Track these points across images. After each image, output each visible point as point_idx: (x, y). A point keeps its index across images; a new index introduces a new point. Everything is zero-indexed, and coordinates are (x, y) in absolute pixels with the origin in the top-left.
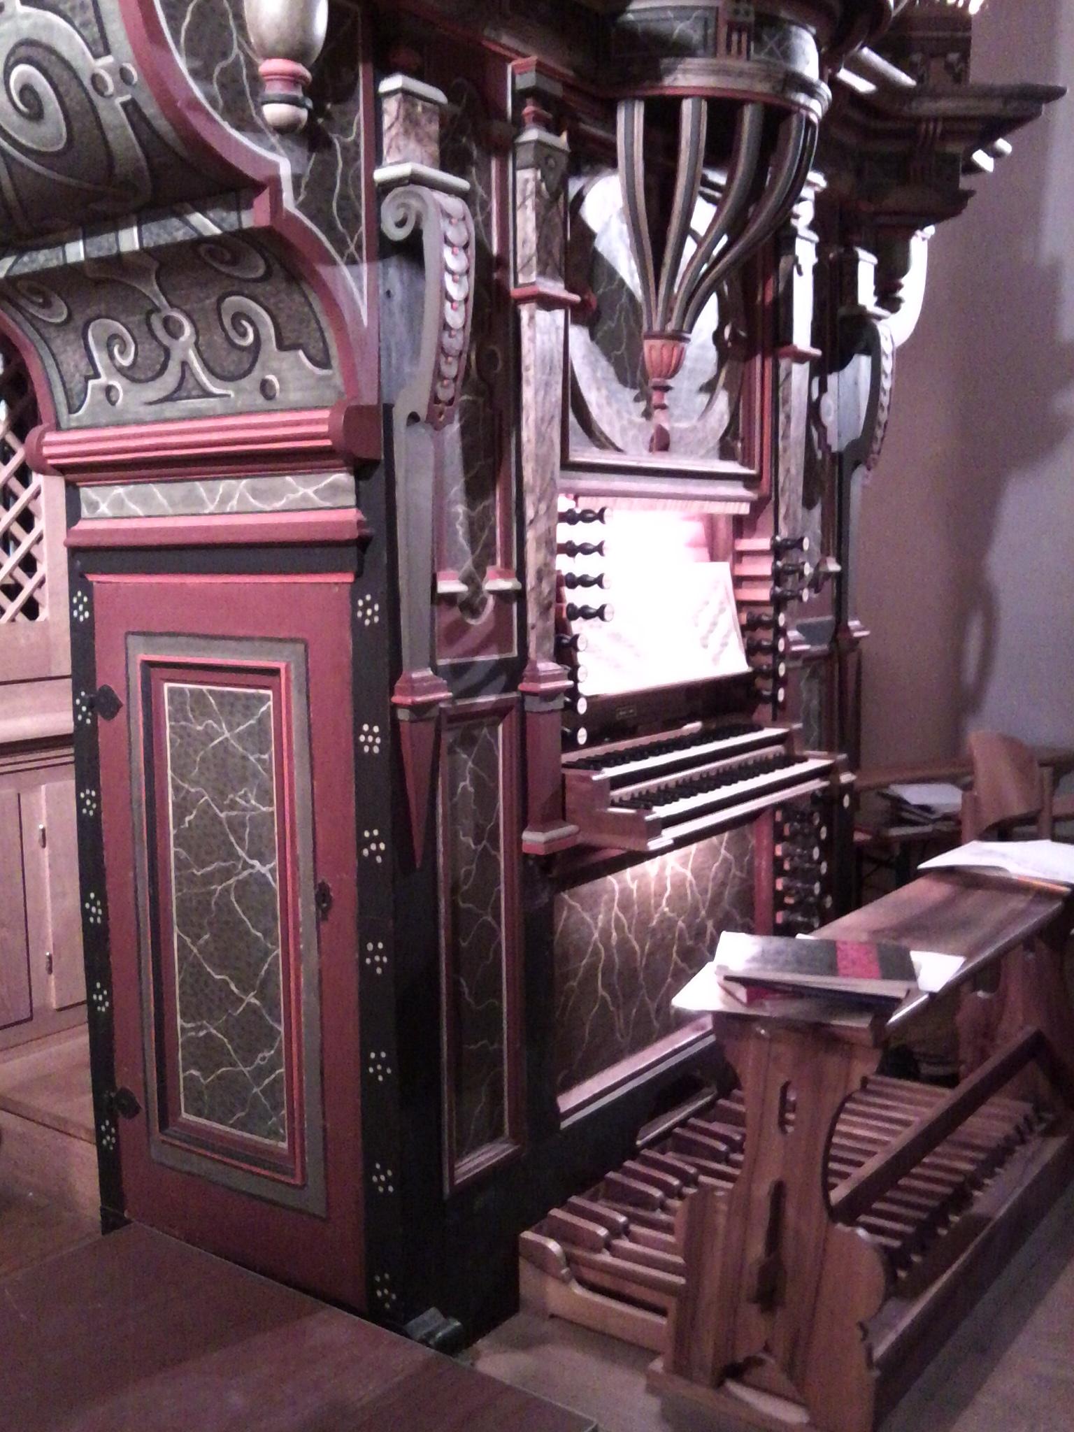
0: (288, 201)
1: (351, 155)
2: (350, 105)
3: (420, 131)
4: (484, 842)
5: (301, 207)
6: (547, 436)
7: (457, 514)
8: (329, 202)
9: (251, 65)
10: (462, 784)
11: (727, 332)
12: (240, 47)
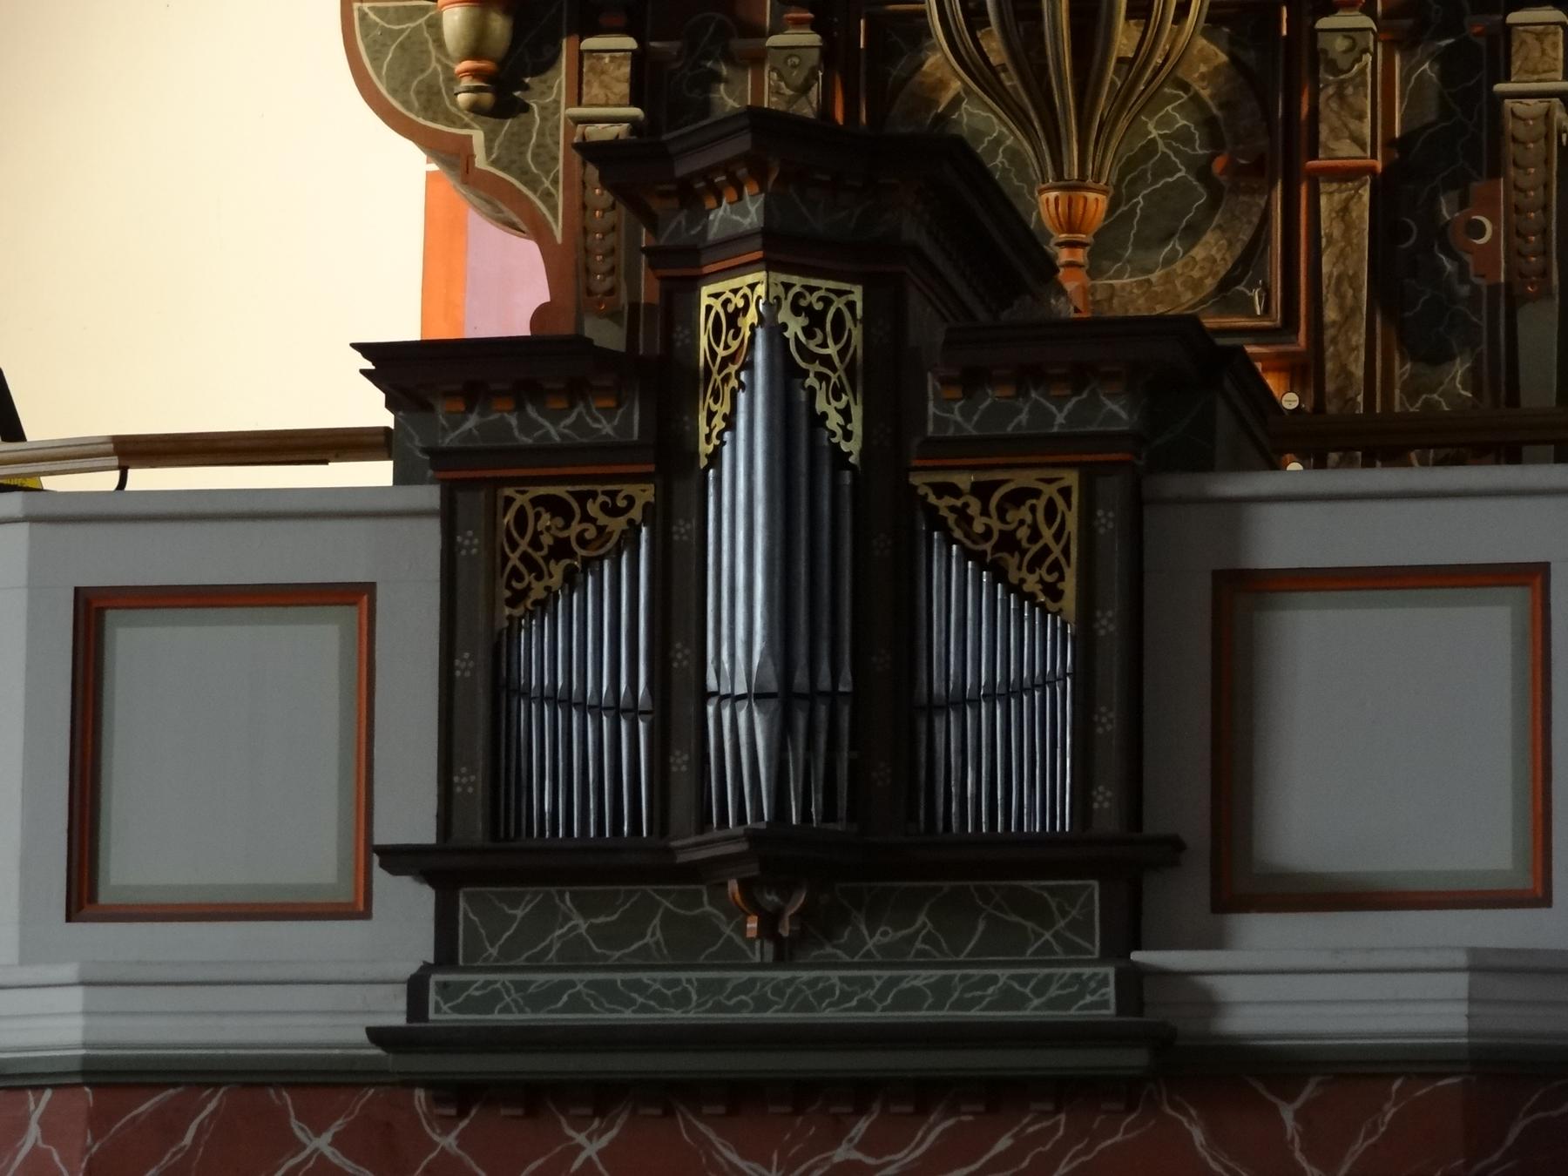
0: (481, 162)
1: (550, 112)
2: (550, 74)
3: (604, 77)
5: (494, 163)
8: (523, 154)
9: (447, 69)
11: (1218, 165)
12: (438, 60)
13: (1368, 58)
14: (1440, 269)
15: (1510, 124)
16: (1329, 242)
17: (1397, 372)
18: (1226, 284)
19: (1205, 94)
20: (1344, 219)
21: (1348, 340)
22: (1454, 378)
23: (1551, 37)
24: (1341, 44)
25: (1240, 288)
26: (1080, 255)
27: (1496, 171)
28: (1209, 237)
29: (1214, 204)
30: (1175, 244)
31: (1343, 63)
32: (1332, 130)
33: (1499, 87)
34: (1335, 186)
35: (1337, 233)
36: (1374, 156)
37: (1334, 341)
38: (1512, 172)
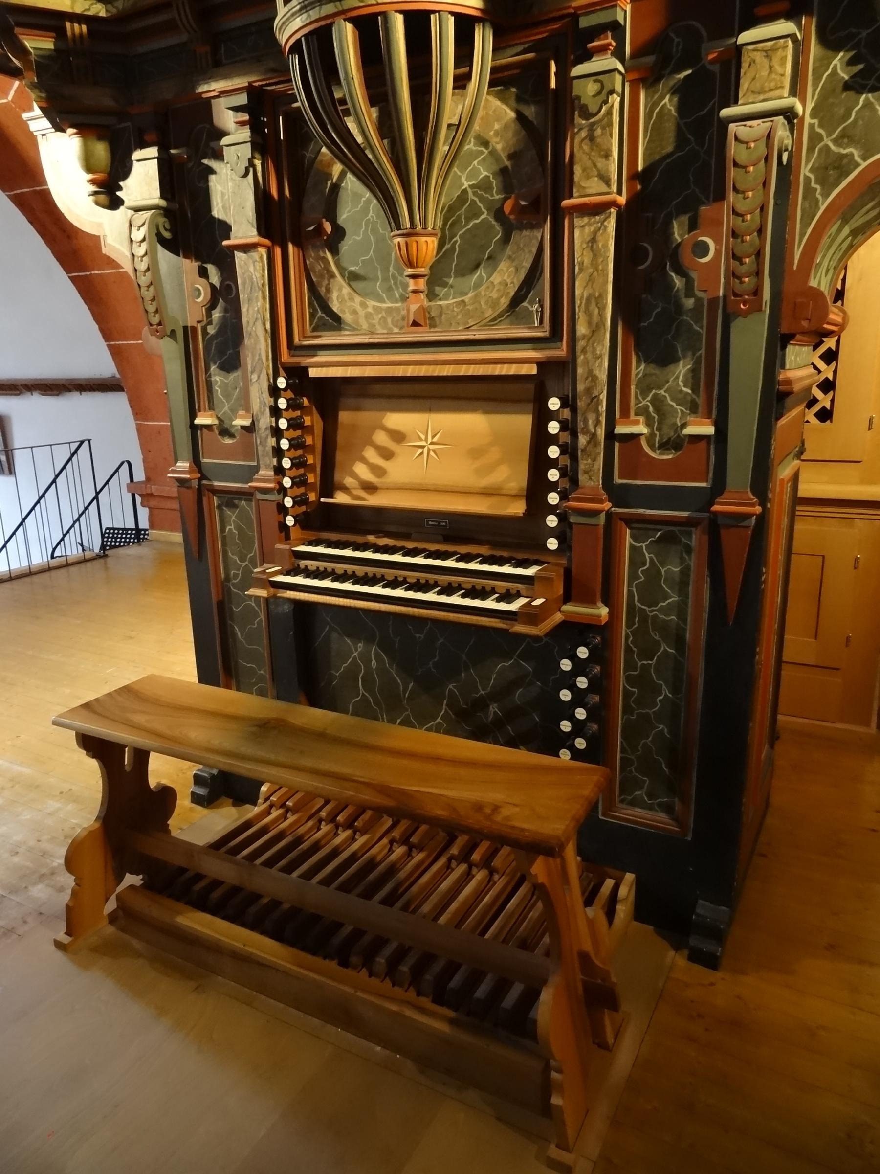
4: (247, 563)
6: (253, 334)
7: (216, 381)
10: (228, 528)
11: (508, 207)
13: (615, 100)
14: (670, 285)
15: (733, 150)
16: (581, 270)
17: (634, 372)
18: (516, 301)
19: (499, 147)
20: (594, 247)
21: (594, 350)
22: (677, 377)
23: (780, 53)
24: (591, 87)
25: (525, 304)
26: (422, 284)
27: (720, 196)
28: (503, 265)
29: (506, 239)
30: (481, 272)
31: (593, 109)
32: (584, 170)
33: (725, 112)
34: (586, 220)
35: (587, 261)
36: (620, 192)
37: (584, 350)
38: (731, 196)
